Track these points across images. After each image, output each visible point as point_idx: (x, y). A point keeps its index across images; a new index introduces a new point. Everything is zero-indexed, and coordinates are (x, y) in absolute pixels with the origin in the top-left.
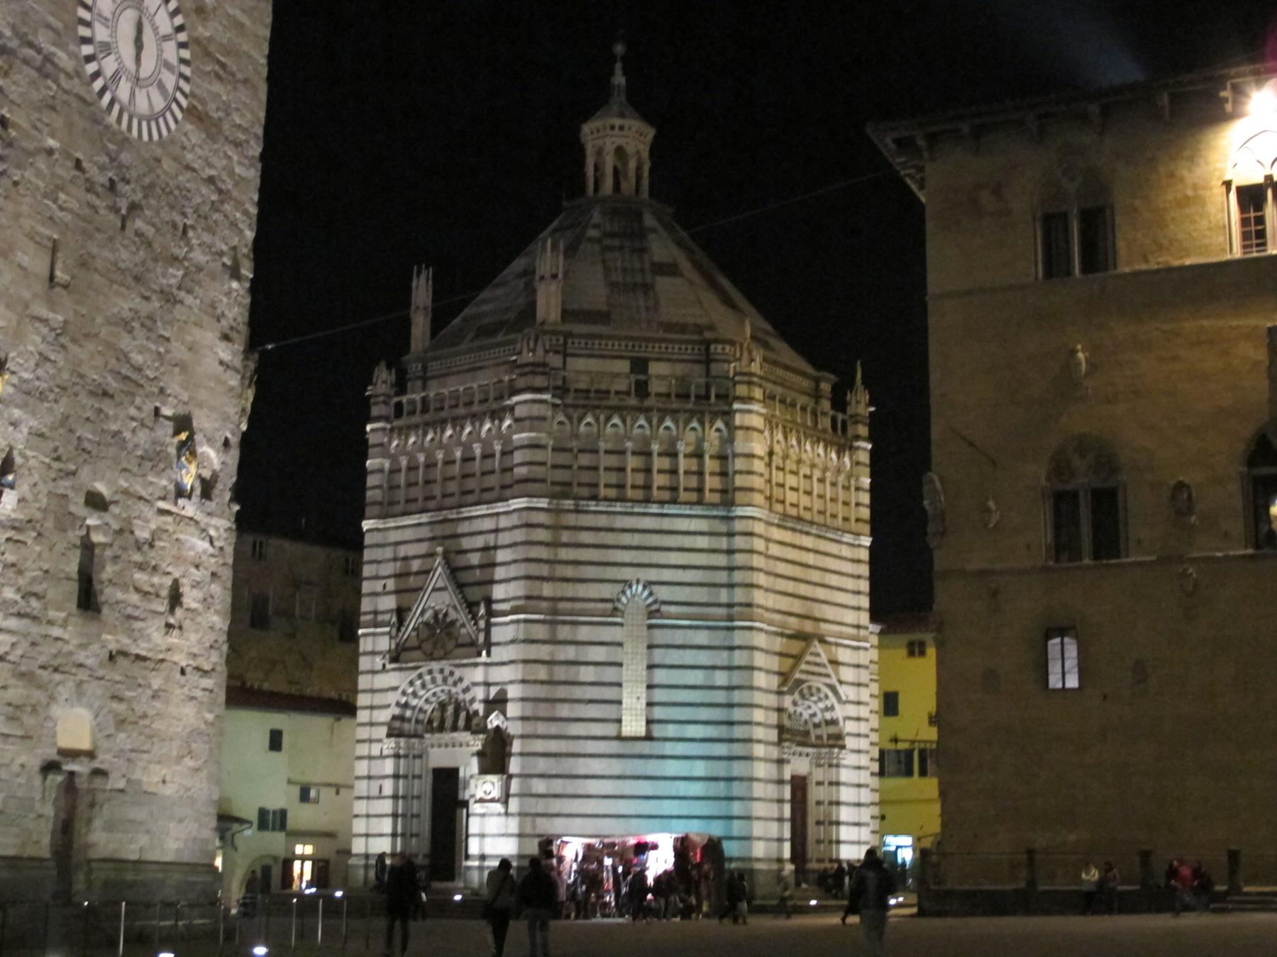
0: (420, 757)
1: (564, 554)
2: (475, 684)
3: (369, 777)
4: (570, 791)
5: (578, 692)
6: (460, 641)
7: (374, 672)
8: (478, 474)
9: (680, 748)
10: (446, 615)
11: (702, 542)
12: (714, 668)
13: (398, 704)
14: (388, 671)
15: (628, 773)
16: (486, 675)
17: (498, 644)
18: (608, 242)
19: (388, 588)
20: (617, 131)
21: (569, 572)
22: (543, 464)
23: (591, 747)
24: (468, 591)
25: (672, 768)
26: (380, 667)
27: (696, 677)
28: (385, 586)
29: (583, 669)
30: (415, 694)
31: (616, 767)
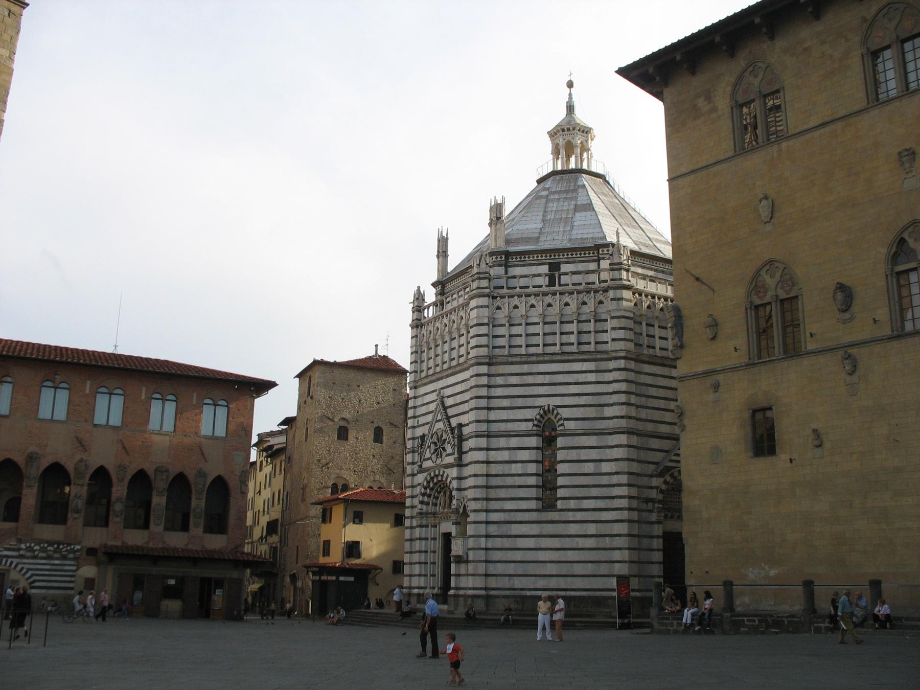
1: (499, 392)
4: (507, 546)
5: (509, 481)
9: (579, 516)
11: (591, 377)
12: (601, 461)
15: (544, 533)
16: (459, 472)
18: (552, 197)
20: (566, 132)
21: (505, 403)
22: (487, 335)
23: (520, 516)
25: (573, 529)
27: (589, 468)
29: (514, 465)
31: (534, 529)
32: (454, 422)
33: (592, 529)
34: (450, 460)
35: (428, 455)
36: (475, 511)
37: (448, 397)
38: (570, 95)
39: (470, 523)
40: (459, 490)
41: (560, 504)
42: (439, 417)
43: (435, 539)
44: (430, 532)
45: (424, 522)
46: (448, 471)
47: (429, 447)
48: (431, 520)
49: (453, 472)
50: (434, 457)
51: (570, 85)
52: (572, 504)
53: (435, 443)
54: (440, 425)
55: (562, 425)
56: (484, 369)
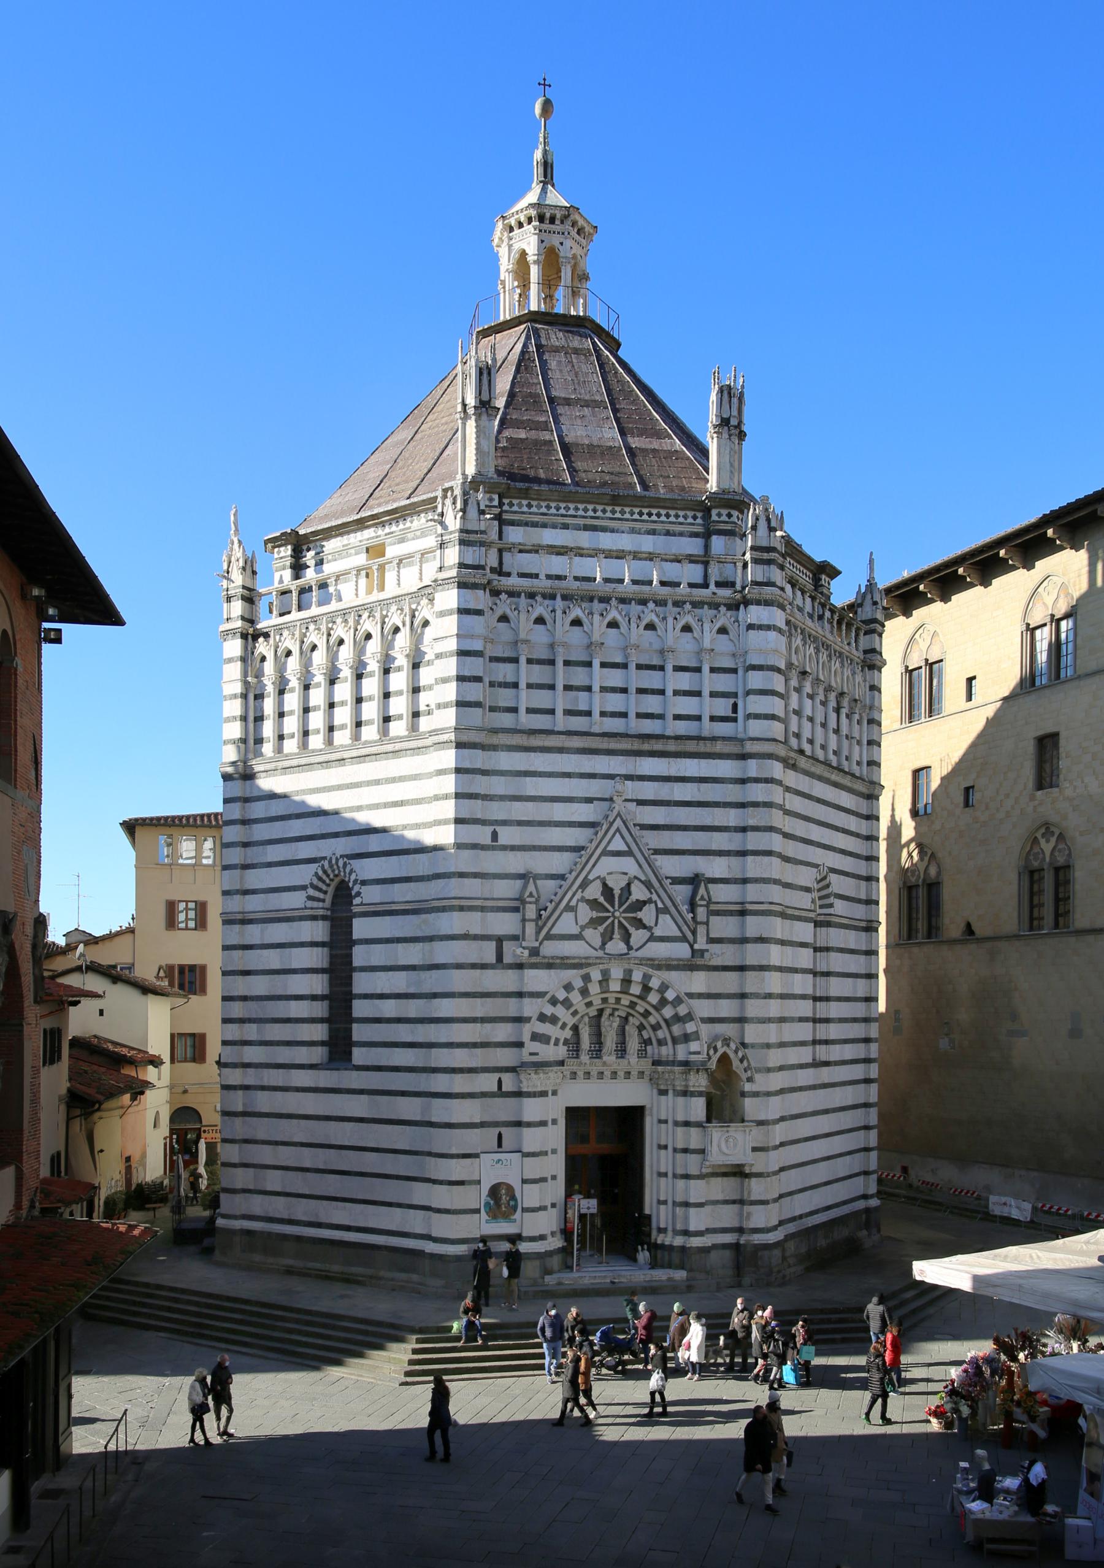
0: (555, 1093)
2: (690, 995)
6: (658, 932)
7: (484, 966)
13: (542, 1018)
14: (520, 966)
19: (502, 840)
26: (491, 958)
28: (495, 836)
30: (567, 1004)
32: (670, 866)
34: (682, 951)
35: (566, 924)
37: (641, 803)
39: (756, 1094)
42: (618, 844)
46: (673, 976)
49: (699, 982)
50: (594, 936)
53: (594, 904)
54: (629, 865)
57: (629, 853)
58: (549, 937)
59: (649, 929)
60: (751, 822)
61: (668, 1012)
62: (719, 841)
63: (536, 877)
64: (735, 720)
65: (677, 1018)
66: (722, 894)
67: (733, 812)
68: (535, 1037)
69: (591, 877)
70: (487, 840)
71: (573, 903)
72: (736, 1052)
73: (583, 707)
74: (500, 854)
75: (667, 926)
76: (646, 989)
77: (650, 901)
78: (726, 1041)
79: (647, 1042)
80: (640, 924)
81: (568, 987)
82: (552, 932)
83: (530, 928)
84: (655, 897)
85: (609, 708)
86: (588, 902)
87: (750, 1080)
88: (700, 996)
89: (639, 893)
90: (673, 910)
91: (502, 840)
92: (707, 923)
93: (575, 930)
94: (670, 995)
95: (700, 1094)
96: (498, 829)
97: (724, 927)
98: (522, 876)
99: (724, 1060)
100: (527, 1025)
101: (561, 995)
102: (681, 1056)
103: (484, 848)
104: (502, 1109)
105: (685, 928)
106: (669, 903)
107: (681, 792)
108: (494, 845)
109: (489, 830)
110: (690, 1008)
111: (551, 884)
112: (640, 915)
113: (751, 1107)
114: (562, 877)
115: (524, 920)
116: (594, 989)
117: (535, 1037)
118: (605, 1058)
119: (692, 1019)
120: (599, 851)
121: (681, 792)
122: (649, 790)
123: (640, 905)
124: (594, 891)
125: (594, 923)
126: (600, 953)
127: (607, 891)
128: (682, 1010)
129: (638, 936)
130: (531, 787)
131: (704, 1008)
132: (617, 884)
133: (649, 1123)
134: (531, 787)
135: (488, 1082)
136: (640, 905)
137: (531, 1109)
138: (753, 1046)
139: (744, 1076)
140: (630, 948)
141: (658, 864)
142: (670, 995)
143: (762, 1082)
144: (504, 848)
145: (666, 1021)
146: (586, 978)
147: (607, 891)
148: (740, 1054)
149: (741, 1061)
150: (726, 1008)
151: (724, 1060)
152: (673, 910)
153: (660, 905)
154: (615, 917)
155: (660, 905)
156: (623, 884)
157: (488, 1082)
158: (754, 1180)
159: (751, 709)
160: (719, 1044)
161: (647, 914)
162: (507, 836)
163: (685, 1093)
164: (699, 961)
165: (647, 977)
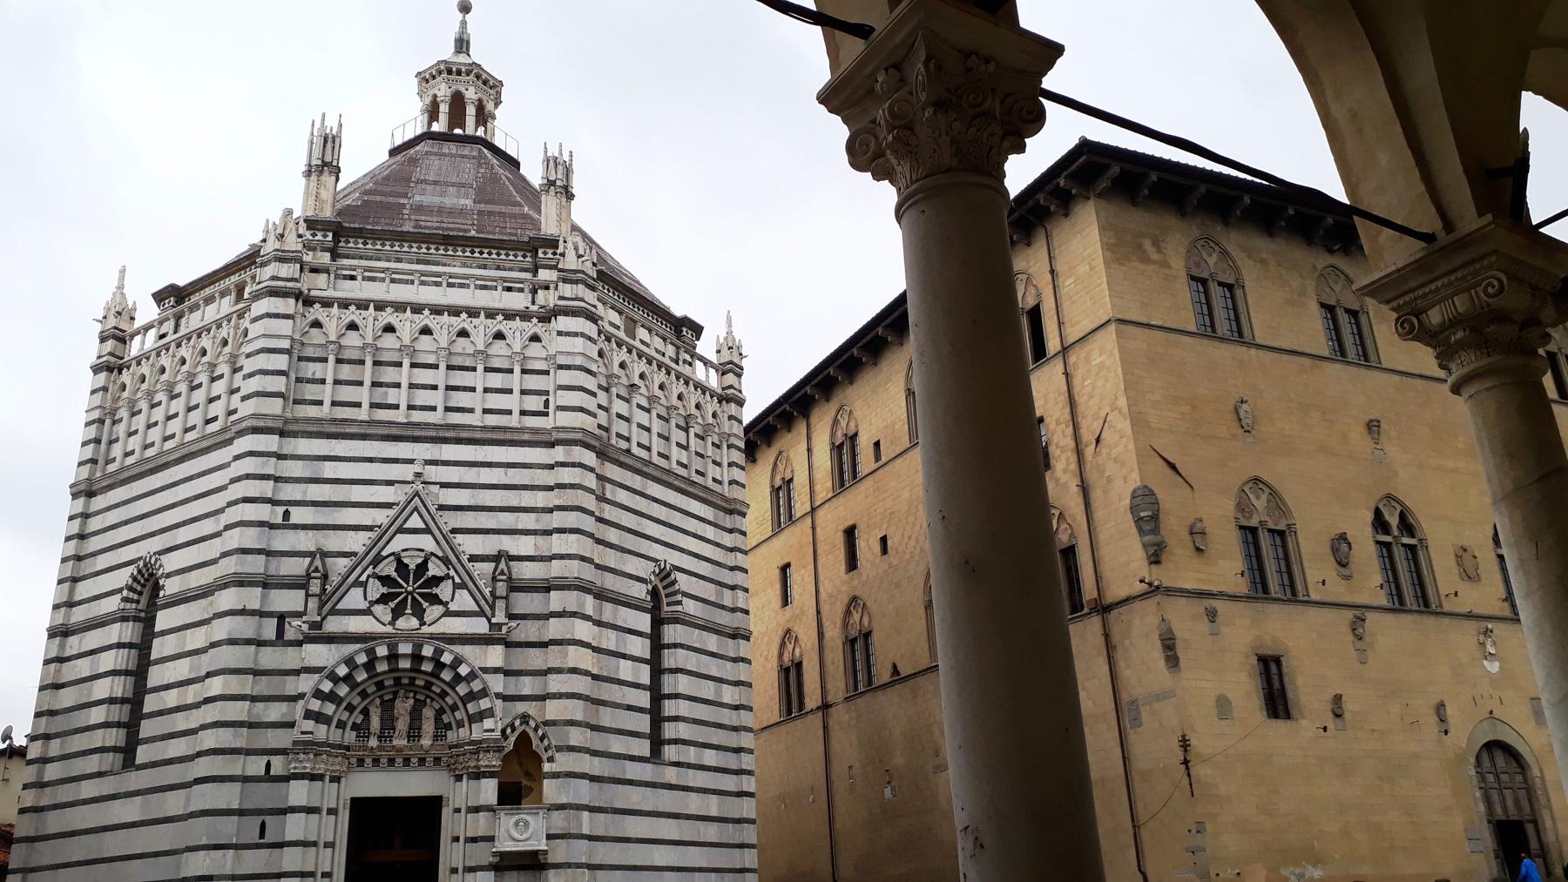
0: (336, 779)
2: (485, 670)
3: (241, 813)
6: (453, 607)
7: (260, 643)
8: (480, 389)
10: (423, 567)
13: (318, 694)
14: (299, 643)
17: (524, 617)
19: (294, 520)
24: (460, 538)
28: (286, 514)
32: (470, 545)
33: (713, 806)
34: (480, 626)
35: (355, 599)
36: (572, 749)
37: (444, 485)
38: (464, 24)
39: (555, 775)
40: (506, 698)
41: (670, 752)
42: (415, 522)
43: (331, 811)
44: (328, 795)
45: (320, 768)
46: (466, 651)
47: (364, 585)
48: (337, 765)
49: (495, 656)
51: (465, 8)
52: (691, 755)
53: (385, 580)
54: (427, 543)
55: (679, 603)
56: (589, 458)
57: (427, 531)
58: (334, 612)
59: (445, 604)
60: (557, 502)
61: (462, 689)
62: (527, 521)
63: (325, 555)
64: (546, 414)
65: (472, 696)
66: (527, 571)
67: (540, 494)
68: (309, 715)
69: (384, 553)
70: (279, 520)
71: (363, 578)
72: (536, 730)
73: (391, 401)
74: (290, 534)
75: (463, 601)
76: (440, 666)
77: (447, 577)
78: (525, 718)
79: (448, 727)
80: (435, 600)
81: (350, 661)
82: (339, 607)
83: (313, 604)
84: (452, 573)
85: (418, 402)
86: (380, 578)
87: (551, 760)
88: (496, 670)
89: (435, 569)
90: (470, 584)
91: (294, 520)
92: (506, 598)
93: (364, 605)
94: (463, 670)
95: (491, 775)
96: (291, 509)
97: (526, 603)
98: (311, 555)
99: (524, 739)
100: (301, 703)
101: (342, 671)
102: (476, 735)
103: (272, 526)
104: (264, 796)
105: (483, 602)
106: (466, 578)
107: (487, 476)
108: (286, 525)
109: (281, 510)
110: (484, 682)
111: (342, 564)
112: (435, 590)
113: (551, 791)
114: (354, 554)
115: (307, 595)
116: (382, 667)
117: (309, 715)
118: (396, 742)
119: (486, 695)
120: (393, 528)
121: (487, 476)
122: (453, 475)
123: (436, 581)
124: (387, 568)
125: (384, 599)
126: (389, 629)
127: (401, 567)
128: (476, 686)
129: (433, 612)
130: (330, 469)
131: (497, 684)
132: (412, 562)
133: (446, 813)
134: (330, 469)
135: (256, 766)
136: (436, 581)
137: (299, 793)
138: (553, 723)
139: (545, 757)
140: (423, 624)
141: (456, 541)
142: (463, 670)
143: (564, 762)
144: (296, 527)
145: (461, 698)
146: (371, 652)
147: (401, 567)
148: (540, 733)
149: (542, 739)
150: (527, 686)
151: (524, 739)
152: (470, 584)
153: (457, 580)
154: (410, 593)
155: (457, 580)
156: (419, 561)
157: (256, 766)
158: (551, 872)
159: (561, 403)
160: (517, 723)
161: (444, 591)
162: (299, 515)
163: (477, 775)
164: (496, 634)
165: (438, 652)
